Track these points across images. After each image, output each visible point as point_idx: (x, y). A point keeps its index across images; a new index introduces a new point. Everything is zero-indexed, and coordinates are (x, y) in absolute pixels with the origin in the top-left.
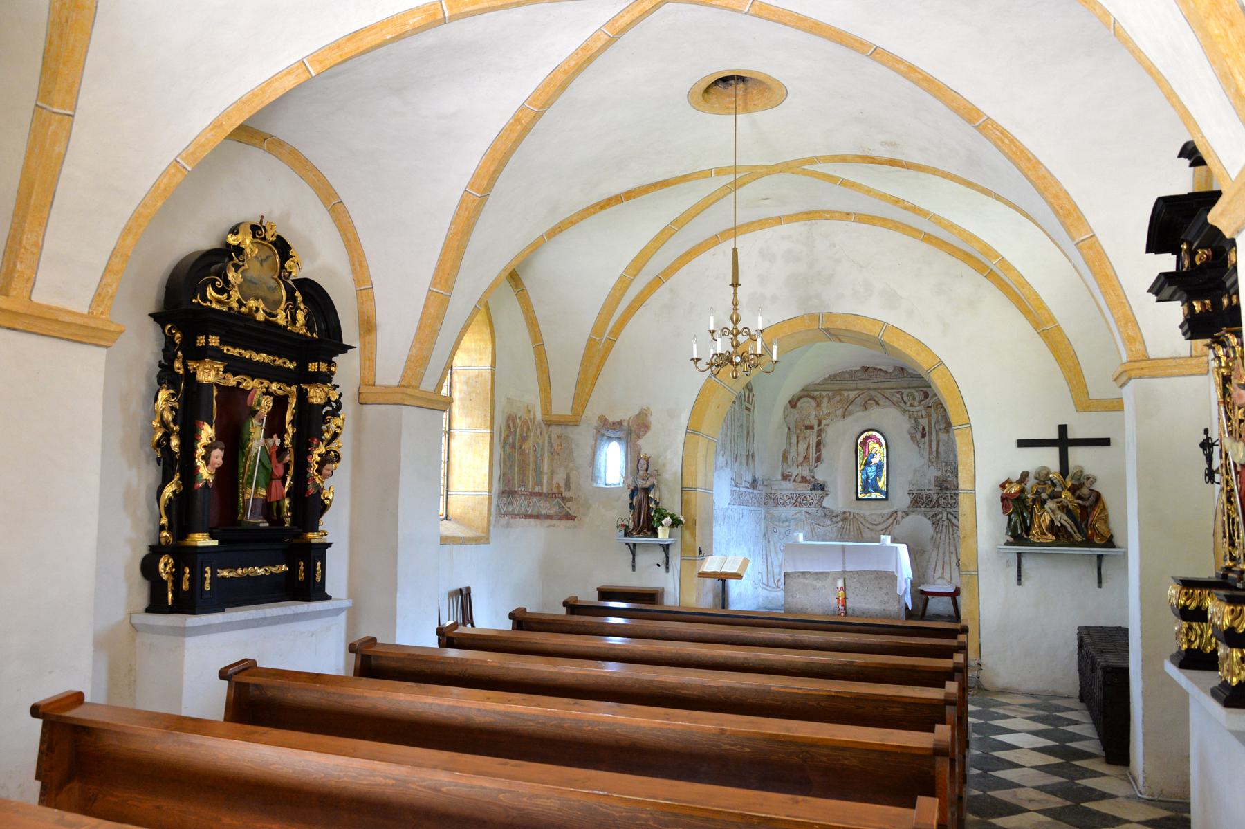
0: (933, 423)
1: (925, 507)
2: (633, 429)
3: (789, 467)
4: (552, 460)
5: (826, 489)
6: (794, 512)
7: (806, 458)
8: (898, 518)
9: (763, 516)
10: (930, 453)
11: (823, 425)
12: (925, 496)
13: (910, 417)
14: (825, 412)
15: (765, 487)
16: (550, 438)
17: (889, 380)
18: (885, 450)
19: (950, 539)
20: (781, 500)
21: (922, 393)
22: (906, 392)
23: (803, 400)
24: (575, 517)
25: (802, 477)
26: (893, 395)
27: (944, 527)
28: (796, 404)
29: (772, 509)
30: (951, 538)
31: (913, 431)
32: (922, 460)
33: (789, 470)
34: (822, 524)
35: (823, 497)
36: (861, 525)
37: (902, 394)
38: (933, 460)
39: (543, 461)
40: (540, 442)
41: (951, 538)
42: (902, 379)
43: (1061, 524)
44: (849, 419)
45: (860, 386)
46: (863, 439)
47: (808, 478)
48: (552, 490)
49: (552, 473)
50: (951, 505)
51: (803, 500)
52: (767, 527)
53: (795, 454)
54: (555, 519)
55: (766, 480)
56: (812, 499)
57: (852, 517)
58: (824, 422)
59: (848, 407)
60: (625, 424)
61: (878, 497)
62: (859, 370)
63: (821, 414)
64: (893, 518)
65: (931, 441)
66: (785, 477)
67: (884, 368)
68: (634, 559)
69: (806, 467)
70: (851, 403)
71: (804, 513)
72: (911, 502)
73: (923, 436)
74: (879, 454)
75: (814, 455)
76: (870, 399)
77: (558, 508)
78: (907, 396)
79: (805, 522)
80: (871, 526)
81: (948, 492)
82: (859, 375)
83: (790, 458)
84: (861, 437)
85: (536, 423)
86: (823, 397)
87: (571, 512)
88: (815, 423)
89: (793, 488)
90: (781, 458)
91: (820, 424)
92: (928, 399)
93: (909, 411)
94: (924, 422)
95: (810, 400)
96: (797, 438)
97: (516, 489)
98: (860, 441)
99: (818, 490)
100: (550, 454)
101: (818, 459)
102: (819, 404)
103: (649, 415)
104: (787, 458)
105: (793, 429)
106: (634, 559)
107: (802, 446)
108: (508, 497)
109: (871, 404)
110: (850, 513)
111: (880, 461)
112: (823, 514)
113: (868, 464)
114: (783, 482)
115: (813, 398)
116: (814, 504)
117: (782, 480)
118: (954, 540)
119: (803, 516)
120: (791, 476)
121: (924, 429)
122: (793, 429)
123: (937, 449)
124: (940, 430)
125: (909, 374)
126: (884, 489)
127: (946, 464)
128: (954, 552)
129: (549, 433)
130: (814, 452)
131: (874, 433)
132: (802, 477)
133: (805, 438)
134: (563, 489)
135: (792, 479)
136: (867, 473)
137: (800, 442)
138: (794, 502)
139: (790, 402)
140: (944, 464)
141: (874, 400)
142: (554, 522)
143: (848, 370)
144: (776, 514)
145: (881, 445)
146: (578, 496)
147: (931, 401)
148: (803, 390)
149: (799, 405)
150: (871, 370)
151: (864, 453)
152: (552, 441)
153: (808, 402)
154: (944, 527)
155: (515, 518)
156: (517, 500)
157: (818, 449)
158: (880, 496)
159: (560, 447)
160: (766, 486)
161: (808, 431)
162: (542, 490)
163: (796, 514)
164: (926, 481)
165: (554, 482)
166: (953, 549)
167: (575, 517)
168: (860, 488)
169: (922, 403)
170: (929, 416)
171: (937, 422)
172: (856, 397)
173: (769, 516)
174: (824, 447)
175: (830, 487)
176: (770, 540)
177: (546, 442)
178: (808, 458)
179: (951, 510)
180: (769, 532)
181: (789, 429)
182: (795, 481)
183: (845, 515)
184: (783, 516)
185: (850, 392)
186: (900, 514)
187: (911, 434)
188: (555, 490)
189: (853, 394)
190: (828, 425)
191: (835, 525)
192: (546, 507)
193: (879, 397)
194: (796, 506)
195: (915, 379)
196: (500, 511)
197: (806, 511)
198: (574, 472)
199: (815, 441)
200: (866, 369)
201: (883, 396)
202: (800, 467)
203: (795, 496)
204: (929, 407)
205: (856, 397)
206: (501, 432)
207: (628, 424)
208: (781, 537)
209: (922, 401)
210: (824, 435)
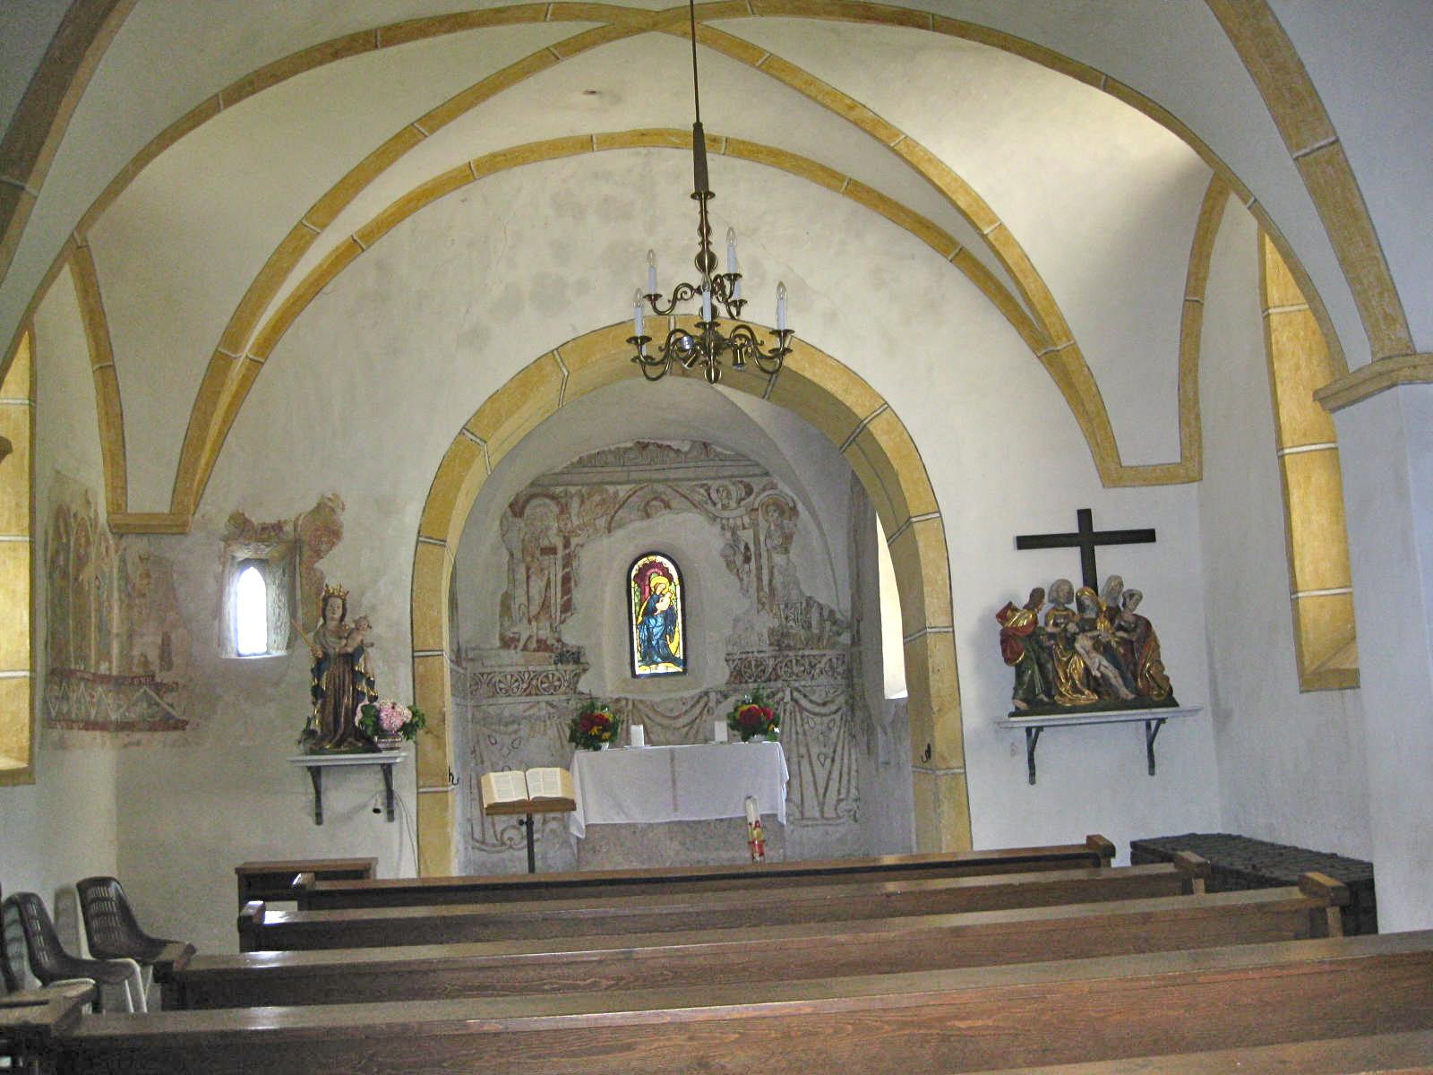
0: (762, 538)
1: (755, 681)
2: (306, 538)
3: (513, 624)
5: (582, 660)
7: (545, 606)
8: (710, 704)
10: (760, 589)
11: (572, 547)
12: (753, 663)
13: (723, 528)
14: (576, 522)
16: (123, 560)
17: (683, 465)
18: (678, 587)
19: (797, 733)
20: (502, 686)
21: (741, 486)
22: (714, 484)
23: (534, 502)
24: (186, 723)
25: (539, 641)
26: (693, 491)
27: (788, 714)
28: (524, 507)
29: (485, 702)
30: (800, 731)
31: (729, 552)
32: (746, 603)
33: (516, 630)
35: (578, 676)
37: (709, 488)
38: (764, 600)
39: (110, 612)
40: (106, 569)
41: (800, 731)
42: (705, 463)
43: (1101, 672)
44: (620, 533)
45: (634, 476)
46: (640, 569)
47: (549, 642)
48: (131, 668)
49: (131, 635)
50: (797, 676)
51: (542, 683)
52: (478, 736)
53: (523, 599)
54: (141, 730)
55: (473, 649)
56: (559, 680)
57: (630, 706)
58: (574, 541)
59: (616, 512)
60: (289, 528)
61: (670, 670)
62: (631, 449)
63: (569, 525)
64: (702, 704)
65: (759, 568)
66: (507, 643)
67: (675, 444)
68: (318, 800)
69: (545, 623)
70: (620, 507)
71: (543, 705)
72: (731, 676)
73: (747, 560)
74: (668, 595)
75: (559, 600)
76: (655, 499)
77: (145, 705)
78: (718, 491)
79: (548, 723)
80: (665, 722)
81: (791, 654)
82: (632, 456)
83: (514, 607)
84: (636, 567)
86: (572, 497)
87: (176, 713)
88: (559, 543)
89: (522, 661)
90: (498, 610)
91: (567, 545)
92: (752, 497)
93: (722, 519)
94: (747, 536)
95: (547, 501)
96: (528, 573)
97: (73, 667)
98: (634, 573)
99: (568, 662)
100: (123, 595)
101: (567, 607)
102: (564, 509)
103: (338, 510)
104: (509, 608)
105: (518, 555)
106: (318, 800)
107: (537, 585)
108: (61, 683)
109: (655, 507)
110: (627, 700)
111: (671, 608)
113: (650, 612)
114: (503, 653)
115: (553, 497)
116: (562, 689)
117: (500, 648)
118: (805, 734)
119: (543, 710)
120: (519, 640)
121: (747, 548)
122: (518, 555)
123: (771, 581)
124: (775, 548)
125: (717, 454)
126: (680, 655)
127: (786, 606)
128: (806, 756)
130: (559, 595)
131: (659, 559)
132: (539, 641)
133: (542, 570)
135: (521, 645)
136: (648, 629)
137: (533, 578)
138: (525, 686)
139: (511, 506)
140: (782, 607)
141: (662, 501)
142: (137, 736)
143: (613, 448)
144: (491, 710)
145: (670, 579)
146: (191, 680)
147: (758, 500)
148: (533, 484)
149: (527, 511)
150: (651, 447)
151: (642, 593)
153: (545, 505)
154: (788, 714)
156: (73, 691)
157: (566, 590)
158: (672, 668)
159: (145, 582)
161: (546, 557)
162: (110, 669)
163: (531, 707)
164: (754, 638)
165: (136, 652)
166: (803, 751)
167: (186, 723)
168: (637, 657)
169: (743, 503)
170: (755, 525)
171: (769, 536)
172: (629, 497)
173: (479, 715)
174: (576, 585)
175: (589, 657)
176: (485, 758)
178: (549, 607)
179: (797, 684)
181: (512, 555)
182: (525, 648)
183: (619, 706)
184: (506, 713)
185: (619, 487)
186: (713, 696)
187: (725, 556)
188: (138, 670)
189: (623, 491)
190: (582, 546)
192: (120, 706)
193: (669, 494)
194: (530, 694)
195: (727, 463)
196: (49, 713)
198: (181, 631)
199: (560, 575)
200: (644, 446)
201: (677, 492)
202: (534, 623)
203: (526, 676)
204: (752, 510)
205: (629, 497)
206: (46, 543)
207: (295, 530)
208: (505, 751)
209: (743, 499)
210: (575, 564)
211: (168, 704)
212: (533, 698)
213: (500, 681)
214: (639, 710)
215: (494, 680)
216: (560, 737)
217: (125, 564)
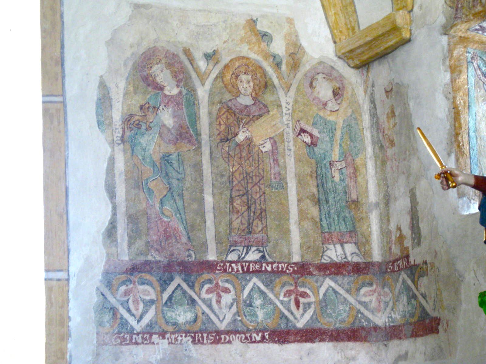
4: (384, 163)
85: (305, 68)
97: (212, 257)
129: (369, 90)
134: (408, 243)
152: (379, 111)
155: (217, 341)
156: (219, 291)
159: (392, 122)
162: (367, 253)
165: (393, 226)
177: (366, 119)
192: (387, 304)
196: (124, 324)
211: (422, 294)
217: (375, 108)
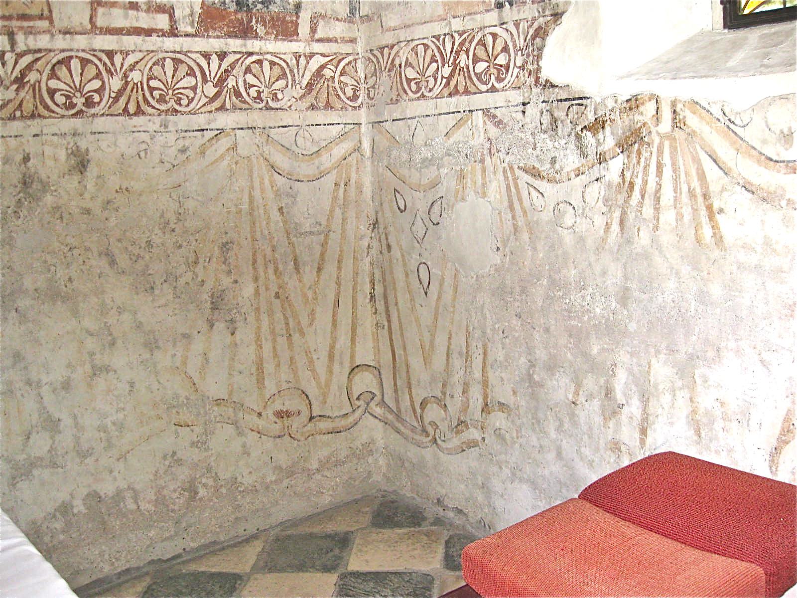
6: (451, 120)
9: (366, 145)
15: (363, 27)
34: (545, 168)
35: (541, 33)
36: (707, 163)
51: (476, 60)
57: (666, 125)
71: (478, 117)
79: (488, 159)
112: (546, 119)
160: (368, 18)
180: (386, 206)
191: (595, 172)
194: (455, 93)
197: (486, 111)
212: (461, 102)
213: (408, 64)
214: (692, 134)
215: (397, 62)
216: (511, 207)
